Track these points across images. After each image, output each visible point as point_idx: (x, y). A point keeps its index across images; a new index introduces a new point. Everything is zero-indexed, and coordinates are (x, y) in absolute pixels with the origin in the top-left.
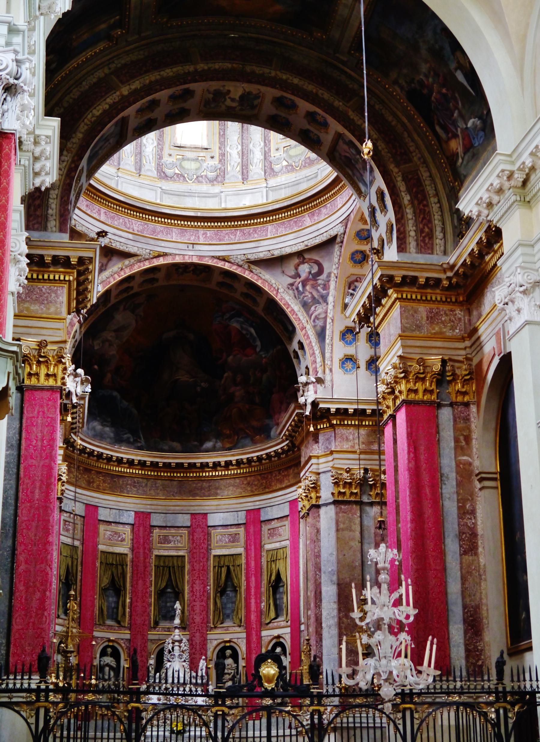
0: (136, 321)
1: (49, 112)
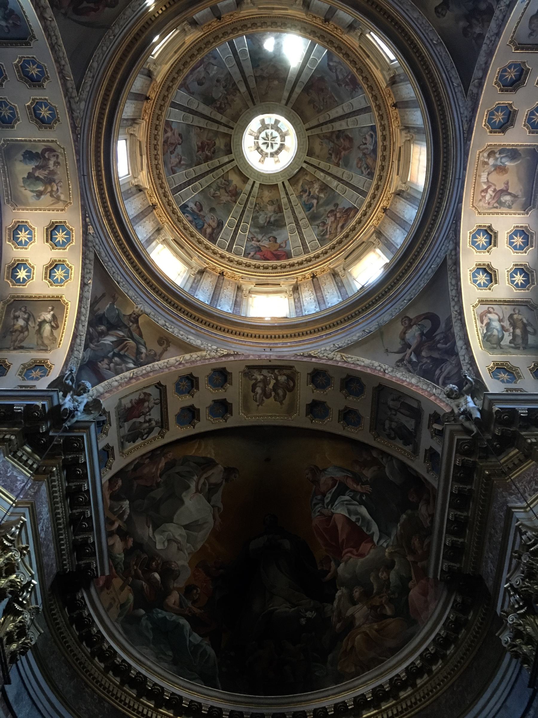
0: (214, 518)
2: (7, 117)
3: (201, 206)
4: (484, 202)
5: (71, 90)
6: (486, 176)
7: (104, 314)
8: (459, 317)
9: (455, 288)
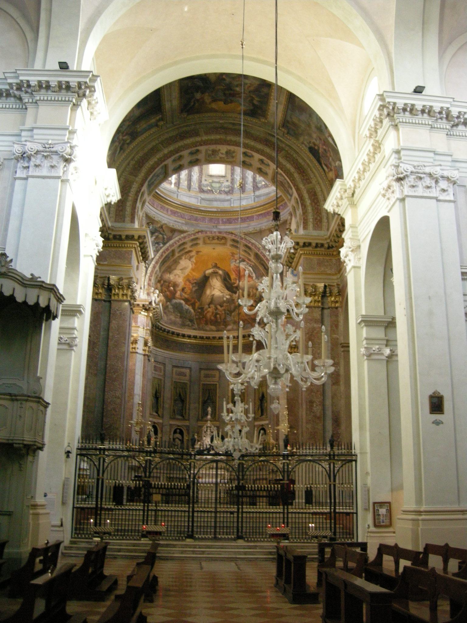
1: (110, 166)
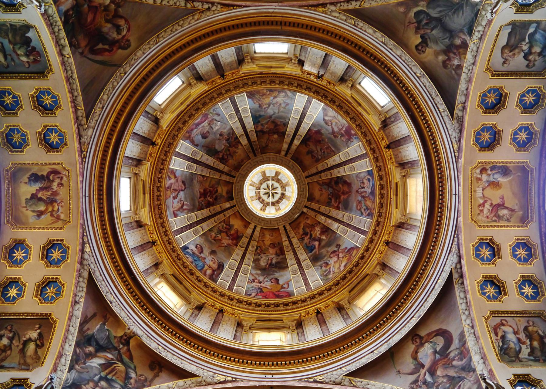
2: (18, 143)
3: (201, 248)
4: (483, 216)
5: (80, 118)
6: (481, 191)
7: (93, 334)
8: (472, 331)
9: (465, 301)
